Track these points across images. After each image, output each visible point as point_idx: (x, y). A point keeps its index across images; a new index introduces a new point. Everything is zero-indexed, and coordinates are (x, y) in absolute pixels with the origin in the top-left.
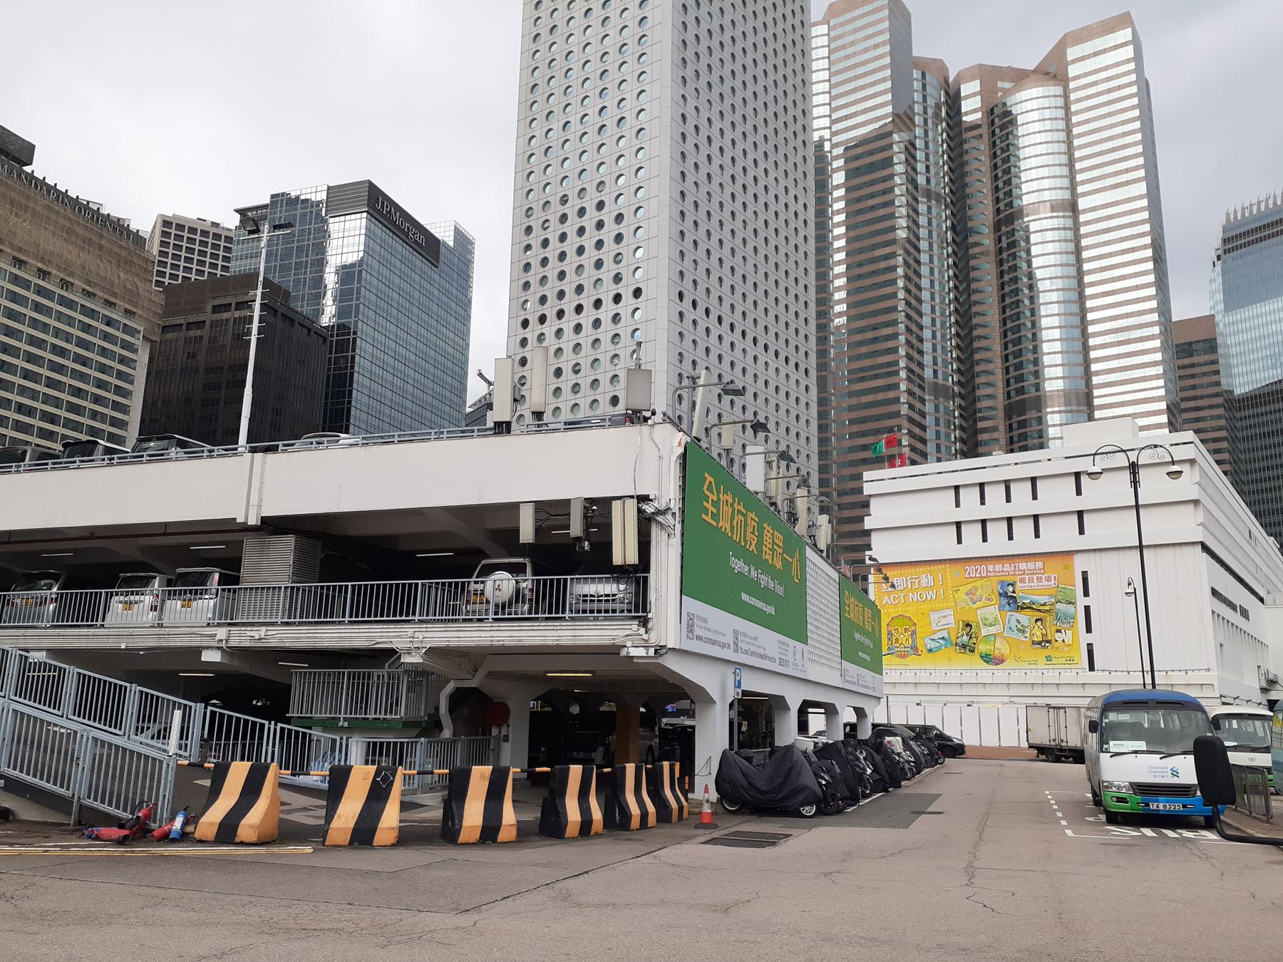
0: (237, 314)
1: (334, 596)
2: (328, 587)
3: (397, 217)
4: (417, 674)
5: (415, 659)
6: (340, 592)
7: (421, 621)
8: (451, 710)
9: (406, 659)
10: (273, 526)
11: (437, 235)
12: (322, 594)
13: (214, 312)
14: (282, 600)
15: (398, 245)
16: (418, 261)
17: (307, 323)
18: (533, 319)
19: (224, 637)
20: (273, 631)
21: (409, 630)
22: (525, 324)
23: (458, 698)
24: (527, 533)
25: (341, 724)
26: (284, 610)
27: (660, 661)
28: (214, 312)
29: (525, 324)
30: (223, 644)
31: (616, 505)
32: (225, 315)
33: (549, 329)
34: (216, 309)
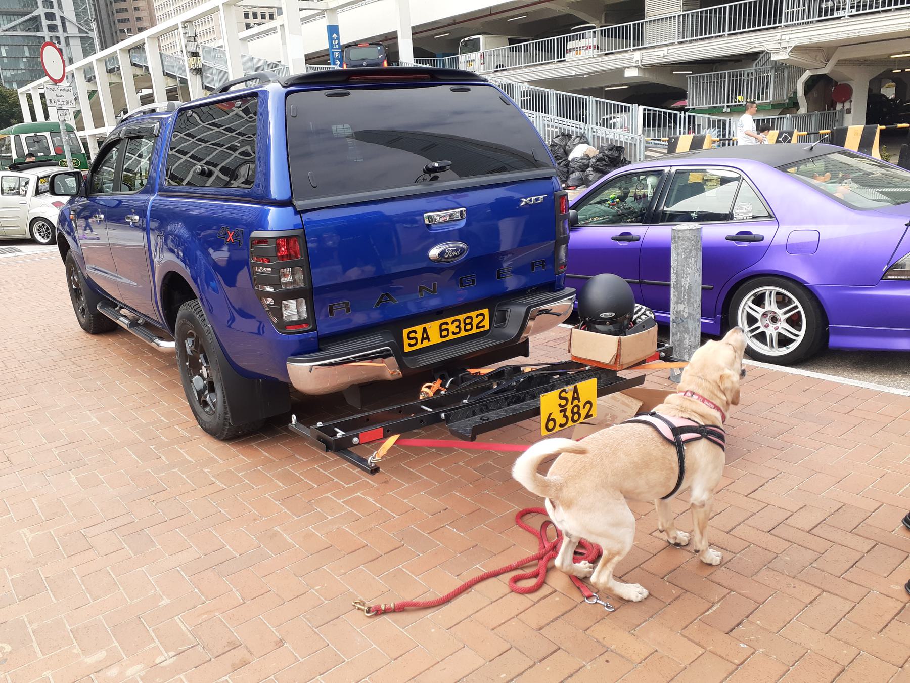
1: (711, 17)
2: (706, 11)
4: (779, 67)
5: (782, 56)
6: (715, 13)
8: (806, 93)
9: (774, 57)
12: (702, 17)
14: (675, 26)
19: (639, 59)
20: (672, 50)
21: (777, 35)
23: (810, 85)
25: (724, 110)
26: (679, 32)
30: (639, 64)
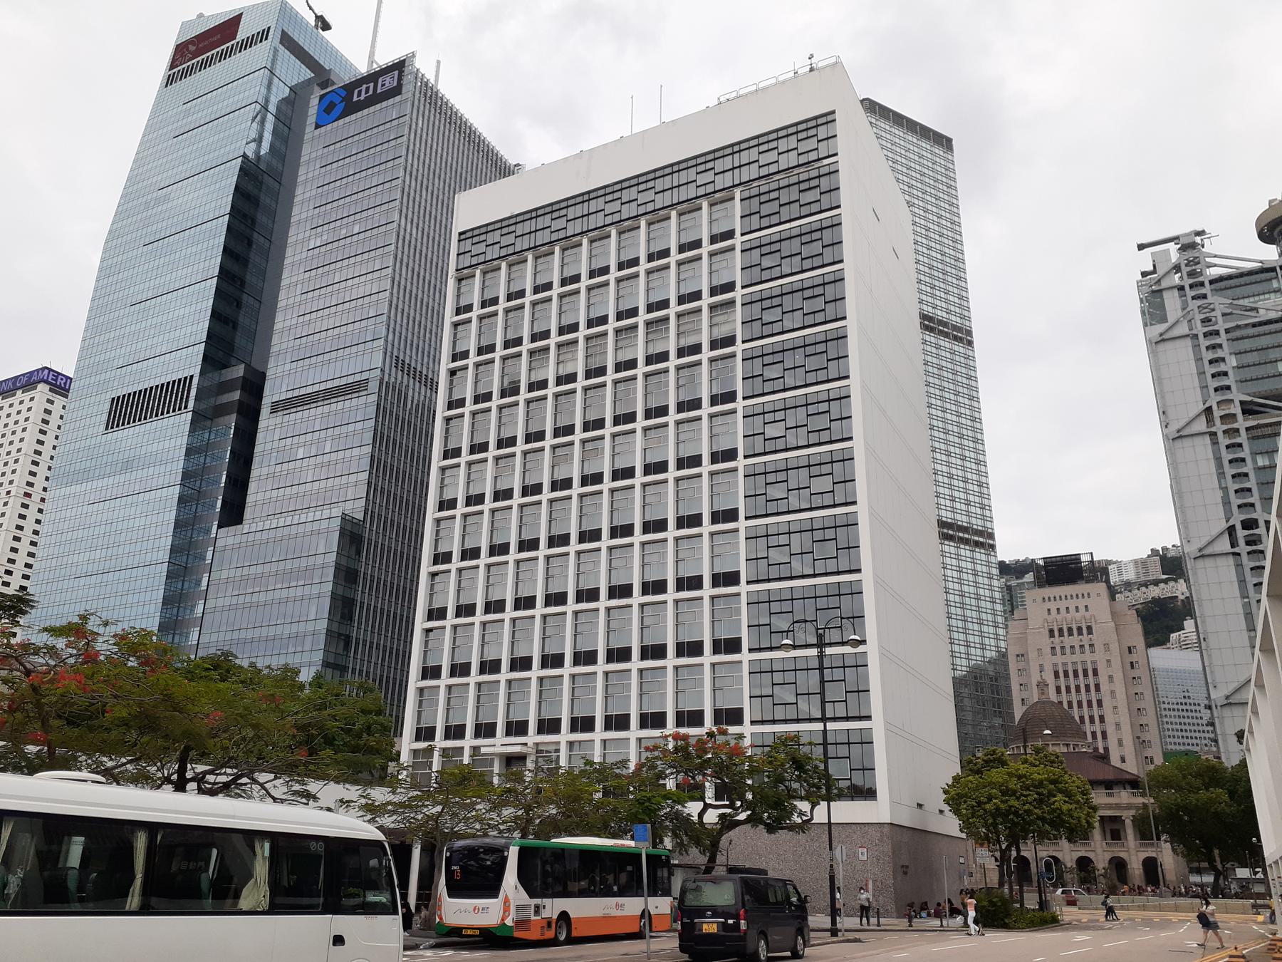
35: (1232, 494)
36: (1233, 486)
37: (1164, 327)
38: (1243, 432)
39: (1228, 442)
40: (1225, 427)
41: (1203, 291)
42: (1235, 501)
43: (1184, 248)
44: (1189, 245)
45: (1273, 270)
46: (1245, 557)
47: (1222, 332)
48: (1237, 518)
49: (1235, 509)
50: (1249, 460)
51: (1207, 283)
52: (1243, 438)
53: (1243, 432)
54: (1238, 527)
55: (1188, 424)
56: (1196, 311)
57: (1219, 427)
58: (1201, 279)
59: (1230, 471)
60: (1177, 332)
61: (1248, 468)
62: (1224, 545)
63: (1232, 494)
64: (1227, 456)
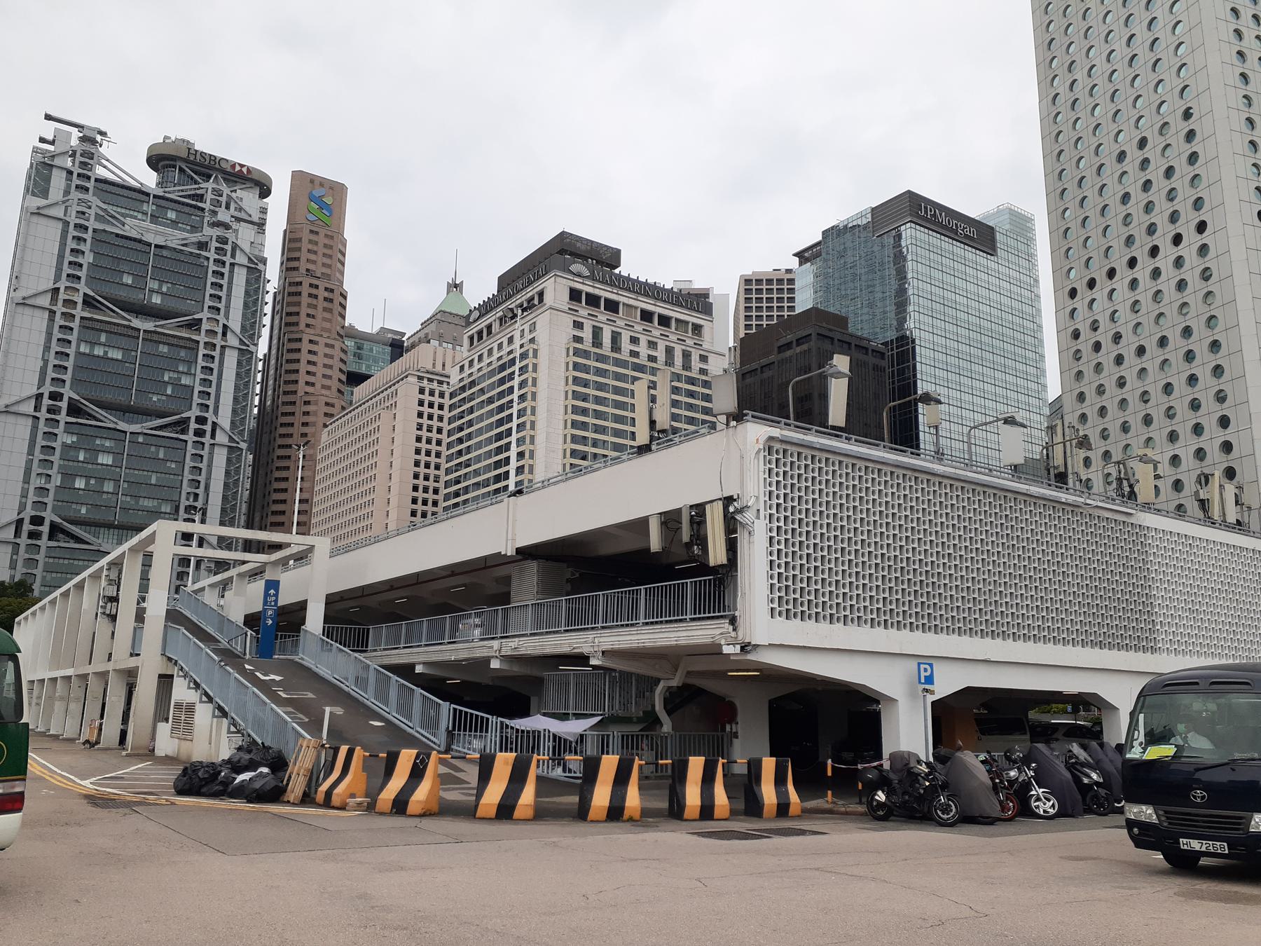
0: (798, 350)
3: (943, 218)
7: (603, 628)
10: (526, 553)
11: (990, 224)
13: (779, 352)
15: (946, 244)
16: (970, 254)
17: (864, 343)
18: (1081, 287)
22: (1073, 293)
24: (655, 543)
27: (750, 657)
28: (779, 352)
29: (1073, 293)
31: (708, 507)
32: (788, 353)
33: (1100, 293)
34: (781, 349)
35: (50, 367)
36: (53, 361)
37: (41, 202)
38: (77, 319)
39: (63, 323)
40: (65, 310)
41: (87, 185)
42: (51, 374)
43: (83, 139)
44: (91, 139)
45: (148, 195)
46: (42, 422)
47: (90, 230)
48: (48, 389)
49: (48, 380)
50: (74, 344)
51: (93, 180)
52: (75, 325)
53: (77, 319)
54: (46, 395)
55: (35, 295)
56: (76, 201)
57: (60, 308)
58: (89, 173)
59: (55, 347)
60: (52, 212)
61: (71, 351)
62: (29, 408)
63: (50, 367)
64: (57, 334)
